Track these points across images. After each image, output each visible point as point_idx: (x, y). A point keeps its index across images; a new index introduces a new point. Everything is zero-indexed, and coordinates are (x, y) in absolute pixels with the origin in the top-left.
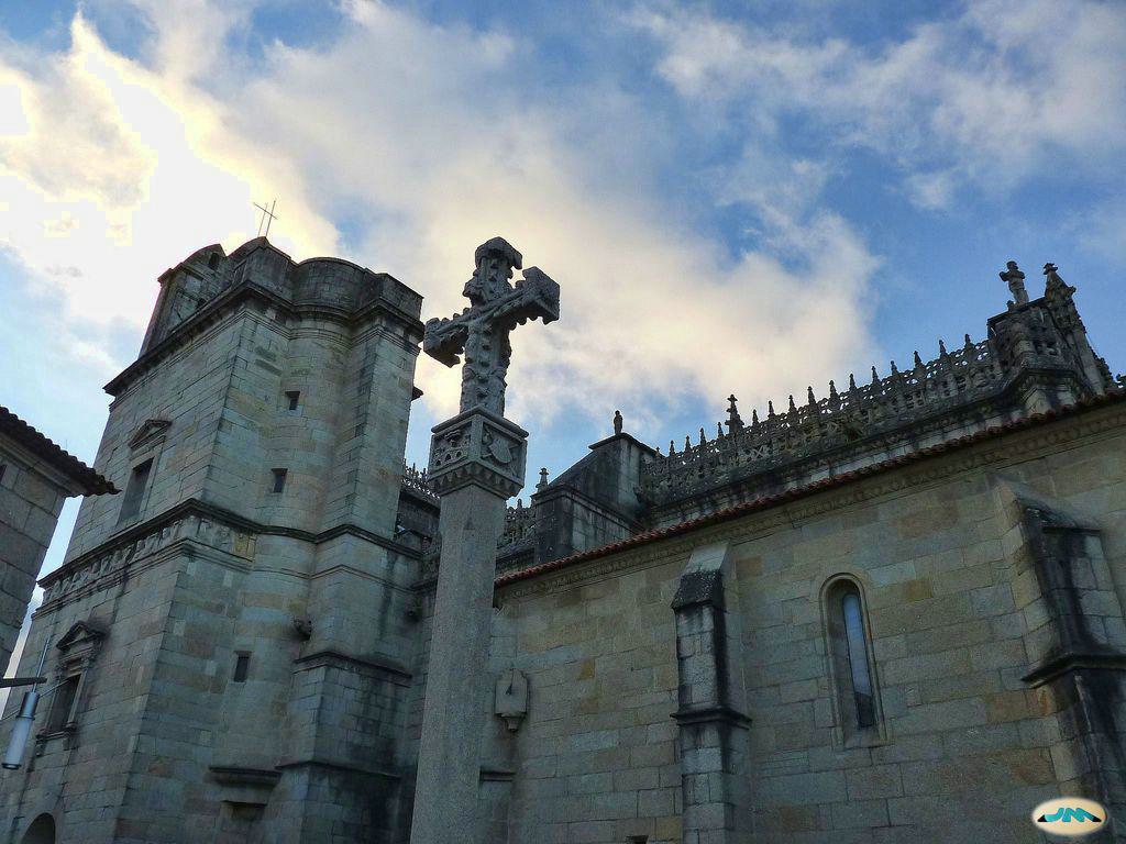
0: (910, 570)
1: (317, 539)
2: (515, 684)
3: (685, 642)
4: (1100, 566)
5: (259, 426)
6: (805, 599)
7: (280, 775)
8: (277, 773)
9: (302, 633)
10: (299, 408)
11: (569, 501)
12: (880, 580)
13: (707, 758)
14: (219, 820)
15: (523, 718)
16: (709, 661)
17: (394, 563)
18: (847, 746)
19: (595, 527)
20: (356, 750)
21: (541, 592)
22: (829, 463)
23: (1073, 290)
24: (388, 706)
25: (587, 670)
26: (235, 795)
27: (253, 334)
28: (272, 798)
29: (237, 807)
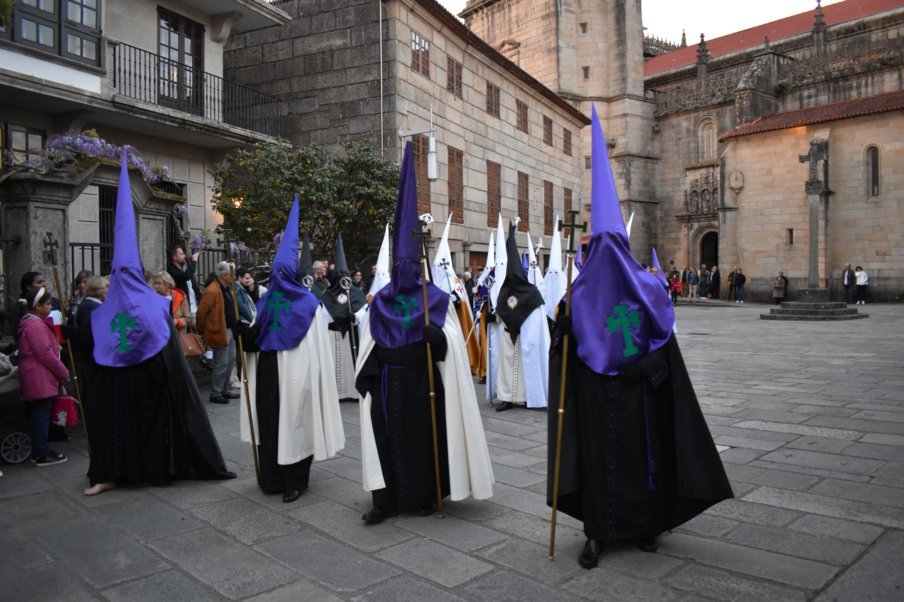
1: (608, 100)
2: (738, 176)
5: (572, 44)
6: (858, 152)
10: (589, 32)
12: (887, 149)
15: (741, 189)
18: (869, 201)
21: (748, 140)
25: (769, 172)
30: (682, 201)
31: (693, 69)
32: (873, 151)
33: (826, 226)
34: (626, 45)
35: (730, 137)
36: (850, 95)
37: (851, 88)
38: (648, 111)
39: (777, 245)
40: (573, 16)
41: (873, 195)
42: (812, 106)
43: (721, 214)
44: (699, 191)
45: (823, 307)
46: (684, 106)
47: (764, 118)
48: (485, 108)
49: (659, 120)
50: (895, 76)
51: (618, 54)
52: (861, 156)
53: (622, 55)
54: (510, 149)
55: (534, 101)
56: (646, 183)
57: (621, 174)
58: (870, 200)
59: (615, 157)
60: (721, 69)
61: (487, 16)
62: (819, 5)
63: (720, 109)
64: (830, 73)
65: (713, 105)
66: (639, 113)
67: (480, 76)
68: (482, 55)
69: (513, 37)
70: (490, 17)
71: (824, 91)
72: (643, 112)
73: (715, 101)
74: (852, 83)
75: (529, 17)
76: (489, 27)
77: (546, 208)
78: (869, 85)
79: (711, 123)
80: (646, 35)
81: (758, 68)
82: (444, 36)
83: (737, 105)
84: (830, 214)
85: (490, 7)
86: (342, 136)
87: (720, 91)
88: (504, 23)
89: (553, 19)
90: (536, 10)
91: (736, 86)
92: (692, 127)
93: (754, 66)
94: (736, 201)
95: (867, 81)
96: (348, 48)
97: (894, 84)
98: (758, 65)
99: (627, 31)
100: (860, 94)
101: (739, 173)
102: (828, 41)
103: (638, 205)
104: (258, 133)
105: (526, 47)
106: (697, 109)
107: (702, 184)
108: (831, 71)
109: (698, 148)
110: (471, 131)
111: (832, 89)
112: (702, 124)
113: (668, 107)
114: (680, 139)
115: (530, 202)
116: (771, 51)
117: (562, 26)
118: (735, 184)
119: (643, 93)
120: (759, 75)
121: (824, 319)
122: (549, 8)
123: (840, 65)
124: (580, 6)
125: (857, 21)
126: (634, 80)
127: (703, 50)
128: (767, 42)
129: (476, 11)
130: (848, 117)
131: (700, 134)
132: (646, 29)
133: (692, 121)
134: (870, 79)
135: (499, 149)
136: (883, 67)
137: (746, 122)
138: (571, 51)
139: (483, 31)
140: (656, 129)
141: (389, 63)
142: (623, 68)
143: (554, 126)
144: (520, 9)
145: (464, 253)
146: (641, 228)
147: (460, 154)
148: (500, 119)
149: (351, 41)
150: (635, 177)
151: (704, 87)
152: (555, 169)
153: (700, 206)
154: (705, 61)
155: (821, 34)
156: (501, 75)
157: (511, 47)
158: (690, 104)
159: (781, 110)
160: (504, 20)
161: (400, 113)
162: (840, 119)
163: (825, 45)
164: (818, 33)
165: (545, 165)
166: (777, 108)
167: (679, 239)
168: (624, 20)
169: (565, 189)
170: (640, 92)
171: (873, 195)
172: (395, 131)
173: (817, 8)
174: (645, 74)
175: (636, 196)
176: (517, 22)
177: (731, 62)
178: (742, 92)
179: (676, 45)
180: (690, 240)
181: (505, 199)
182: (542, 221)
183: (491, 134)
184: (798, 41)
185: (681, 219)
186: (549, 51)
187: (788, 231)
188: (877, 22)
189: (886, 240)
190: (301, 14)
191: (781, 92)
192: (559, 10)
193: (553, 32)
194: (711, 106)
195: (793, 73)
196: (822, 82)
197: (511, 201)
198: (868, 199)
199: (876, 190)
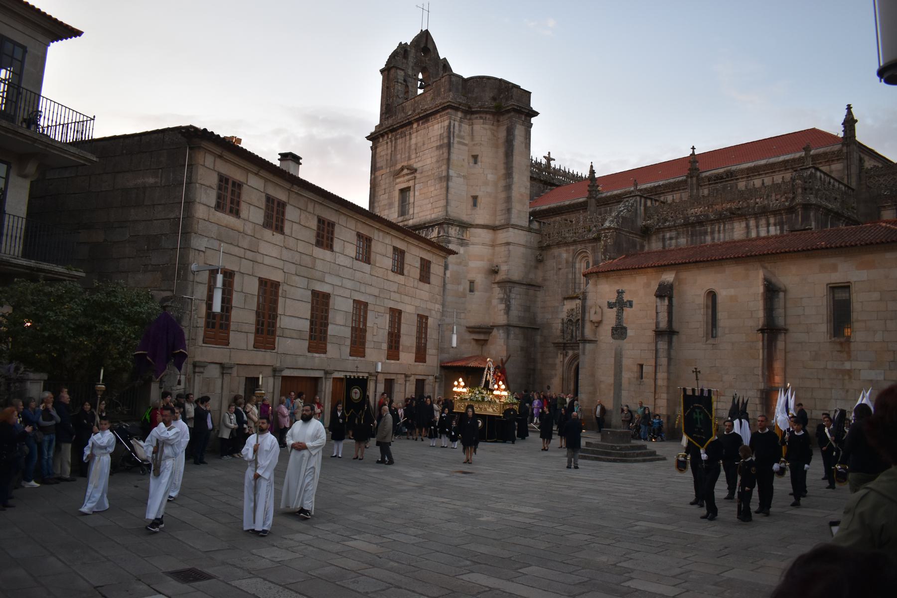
0: (732, 292)
1: (494, 228)
3: (659, 308)
4: (782, 303)
8: (492, 327)
9: (494, 271)
10: (479, 164)
12: (723, 295)
13: (663, 345)
16: (666, 314)
18: (707, 342)
21: (607, 277)
22: (723, 222)
23: (856, 121)
26: (476, 337)
28: (490, 338)
29: (477, 340)
30: (560, 328)
31: (584, 202)
32: (712, 296)
33: (669, 364)
34: (513, 178)
35: (591, 273)
36: (705, 239)
37: (706, 233)
38: (532, 240)
39: (629, 379)
40: (466, 148)
41: (712, 337)
42: (673, 247)
43: (581, 346)
44: (574, 321)
45: (618, 448)
46: (565, 238)
47: (627, 257)
48: (314, 242)
49: (543, 250)
50: (743, 225)
51: (505, 186)
52: (701, 300)
53: (508, 188)
54: (344, 279)
55: (381, 234)
56: (527, 309)
57: (502, 299)
58: (708, 342)
59: (498, 283)
60: (608, 204)
61: (391, 141)
62: (693, 152)
63: (595, 244)
64: (688, 218)
65: (589, 240)
66: (522, 242)
67: (309, 212)
68: (312, 194)
69: (411, 162)
70: (394, 142)
71: (683, 234)
72: (527, 241)
73: (591, 236)
74: (707, 229)
75: (426, 146)
76: (392, 151)
77: (390, 334)
78: (721, 232)
79: (588, 256)
80: (553, 166)
81: (624, 210)
82: (262, 177)
83: (603, 242)
84: (673, 353)
85: (394, 133)
86: (145, 265)
87: (595, 226)
88: (405, 149)
89: (445, 150)
90: (432, 139)
91: (602, 225)
92: (571, 259)
93: (621, 207)
94: (595, 334)
95: (719, 227)
96: (158, 187)
97: (742, 232)
98: (625, 206)
99: (514, 165)
100: (713, 239)
101: (598, 307)
102: (701, 186)
103: (517, 330)
104: (45, 263)
105: (422, 173)
106: (575, 242)
107: (577, 313)
108: (689, 216)
109: (575, 278)
110: (293, 263)
111: (690, 233)
112: (580, 257)
113: (551, 239)
114: (560, 269)
115: (367, 328)
116: (639, 193)
117: (454, 157)
118: (594, 318)
119: (528, 224)
120: (624, 215)
121: (615, 461)
122: (443, 139)
123: (697, 210)
124: (472, 139)
125: (725, 169)
127: (594, 186)
128: (636, 185)
129: (382, 136)
130: (689, 263)
131: (577, 266)
132: (554, 160)
133: (571, 254)
134: (722, 226)
135: (328, 279)
136: (732, 216)
137: (610, 259)
138: (462, 180)
139: (387, 155)
140: (540, 258)
141: (190, 203)
142: (508, 199)
143: (408, 258)
144: (419, 138)
145: (274, 378)
146: (519, 353)
147: (276, 285)
148: (333, 251)
149: (161, 181)
150: (514, 303)
151: (582, 222)
152: (405, 296)
153: (574, 334)
154: (594, 196)
155: (695, 179)
156: (337, 211)
157: (409, 172)
158: (570, 237)
159: (646, 249)
160: (405, 146)
161: (195, 249)
162: (682, 263)
163: (698, 189)
164: (691, 177)
165: (392, 293)
166: (642, 247)
167: (555, 364)
168: (512, 155)
169: (418, 315)
170: (525, 223)
171: (712, 337)
172: (188, 266)
173: (691, 155)
174: (531, 205)
175: (515, 321)
176: (416, 149)
177: (617, 198)
178: (607, 231)
179: (584, 176)
180: (565, 368)
181: (334, 326)
182: (385, 346)
183: (319, 265)
184: (675, 183)
185: (557, 345)
186: (441, 179)
187: (639, 366)
188: (742, 171)
189: (721, 381)
190: (124, 152)
191: (646, 233)
192: (452, 141)
193: (445, 162)
194: (588, 240)
195: (658, 216)
196: (681, 225)
197: (342, 328)
198: (706, 341)
199: (714, 332)
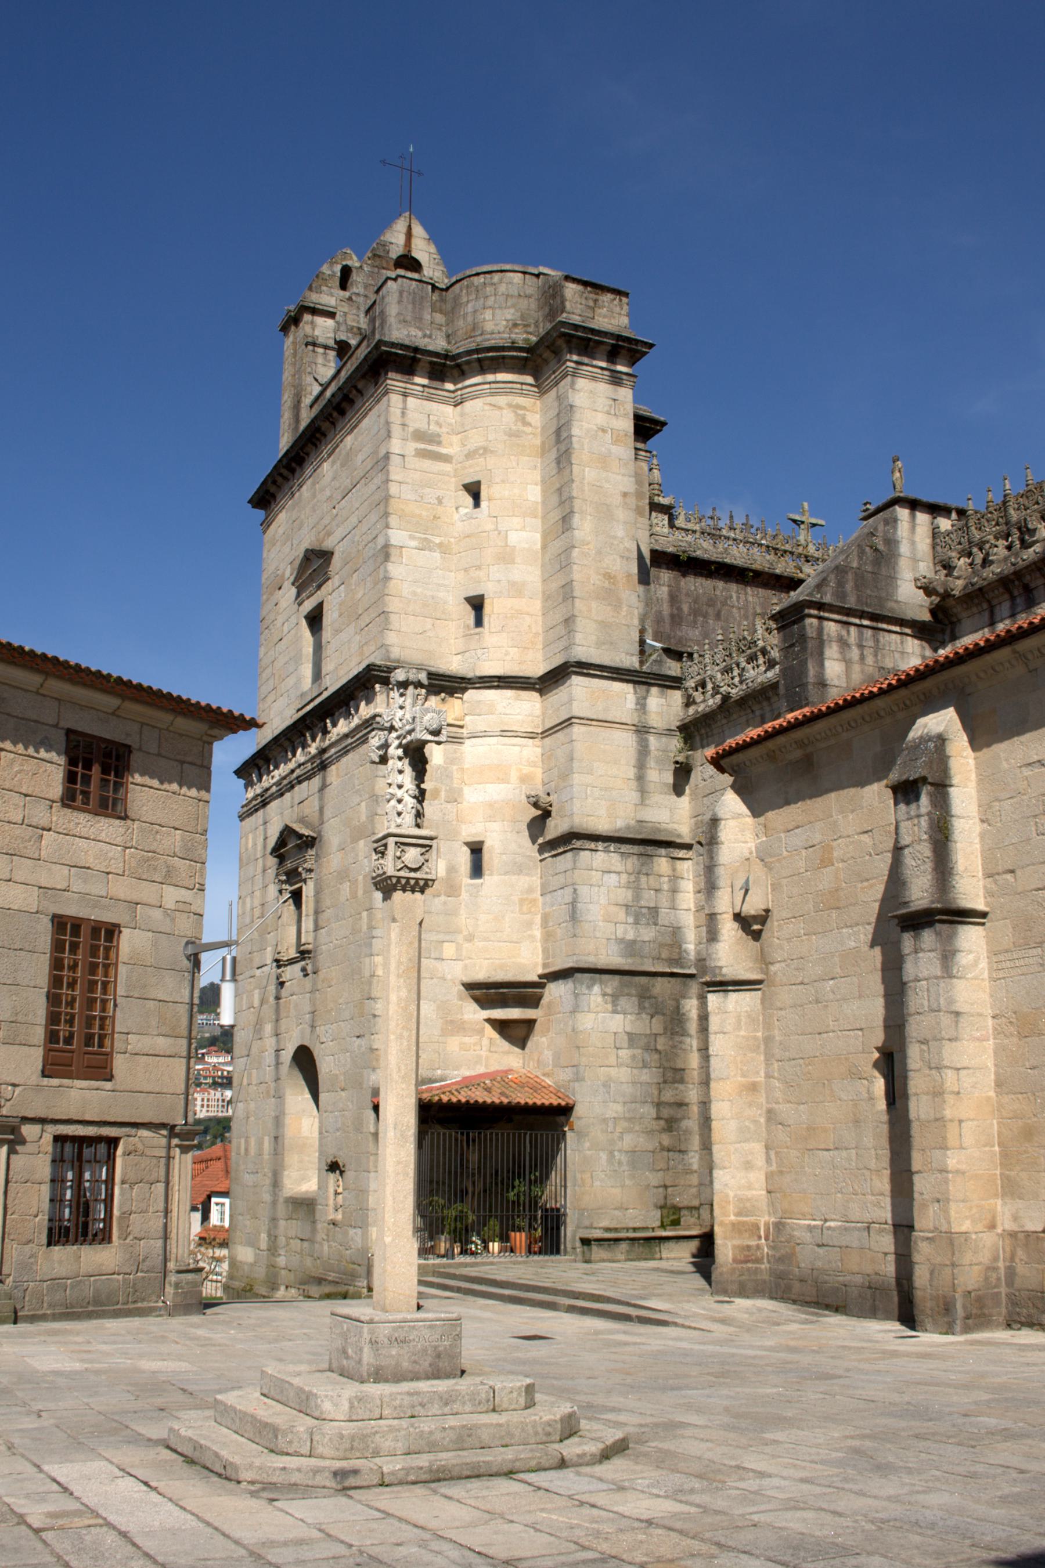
5: (437, 540)
7: (542, 986)
10: (484, 504)
11: (815, 621)
14: (485, 1042)
17: (645, 698)
19: (861, 647)
20: (630, 947)
24: (666, 887)
27: (403, 414)
126: (603, 625)
